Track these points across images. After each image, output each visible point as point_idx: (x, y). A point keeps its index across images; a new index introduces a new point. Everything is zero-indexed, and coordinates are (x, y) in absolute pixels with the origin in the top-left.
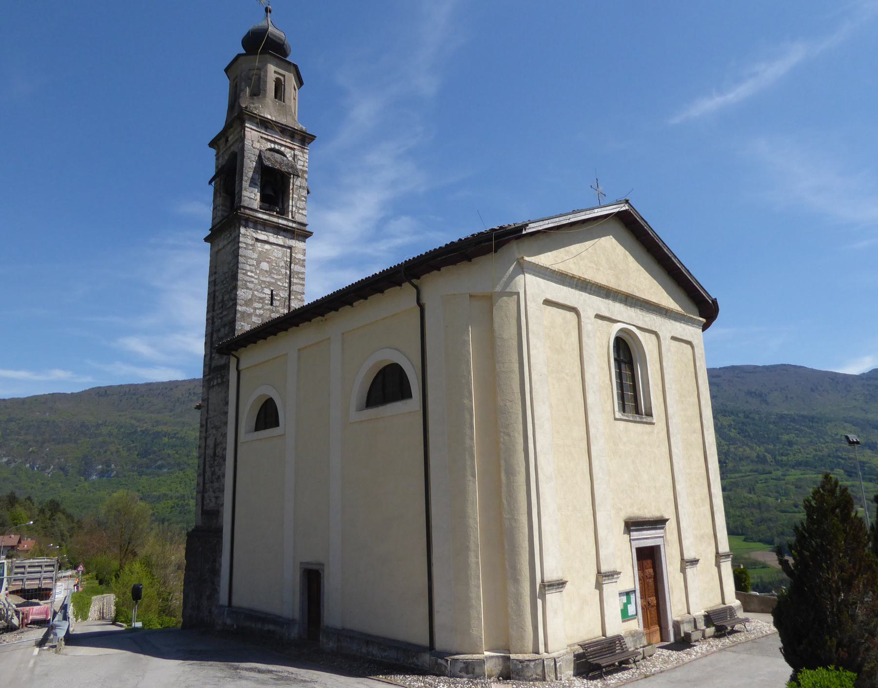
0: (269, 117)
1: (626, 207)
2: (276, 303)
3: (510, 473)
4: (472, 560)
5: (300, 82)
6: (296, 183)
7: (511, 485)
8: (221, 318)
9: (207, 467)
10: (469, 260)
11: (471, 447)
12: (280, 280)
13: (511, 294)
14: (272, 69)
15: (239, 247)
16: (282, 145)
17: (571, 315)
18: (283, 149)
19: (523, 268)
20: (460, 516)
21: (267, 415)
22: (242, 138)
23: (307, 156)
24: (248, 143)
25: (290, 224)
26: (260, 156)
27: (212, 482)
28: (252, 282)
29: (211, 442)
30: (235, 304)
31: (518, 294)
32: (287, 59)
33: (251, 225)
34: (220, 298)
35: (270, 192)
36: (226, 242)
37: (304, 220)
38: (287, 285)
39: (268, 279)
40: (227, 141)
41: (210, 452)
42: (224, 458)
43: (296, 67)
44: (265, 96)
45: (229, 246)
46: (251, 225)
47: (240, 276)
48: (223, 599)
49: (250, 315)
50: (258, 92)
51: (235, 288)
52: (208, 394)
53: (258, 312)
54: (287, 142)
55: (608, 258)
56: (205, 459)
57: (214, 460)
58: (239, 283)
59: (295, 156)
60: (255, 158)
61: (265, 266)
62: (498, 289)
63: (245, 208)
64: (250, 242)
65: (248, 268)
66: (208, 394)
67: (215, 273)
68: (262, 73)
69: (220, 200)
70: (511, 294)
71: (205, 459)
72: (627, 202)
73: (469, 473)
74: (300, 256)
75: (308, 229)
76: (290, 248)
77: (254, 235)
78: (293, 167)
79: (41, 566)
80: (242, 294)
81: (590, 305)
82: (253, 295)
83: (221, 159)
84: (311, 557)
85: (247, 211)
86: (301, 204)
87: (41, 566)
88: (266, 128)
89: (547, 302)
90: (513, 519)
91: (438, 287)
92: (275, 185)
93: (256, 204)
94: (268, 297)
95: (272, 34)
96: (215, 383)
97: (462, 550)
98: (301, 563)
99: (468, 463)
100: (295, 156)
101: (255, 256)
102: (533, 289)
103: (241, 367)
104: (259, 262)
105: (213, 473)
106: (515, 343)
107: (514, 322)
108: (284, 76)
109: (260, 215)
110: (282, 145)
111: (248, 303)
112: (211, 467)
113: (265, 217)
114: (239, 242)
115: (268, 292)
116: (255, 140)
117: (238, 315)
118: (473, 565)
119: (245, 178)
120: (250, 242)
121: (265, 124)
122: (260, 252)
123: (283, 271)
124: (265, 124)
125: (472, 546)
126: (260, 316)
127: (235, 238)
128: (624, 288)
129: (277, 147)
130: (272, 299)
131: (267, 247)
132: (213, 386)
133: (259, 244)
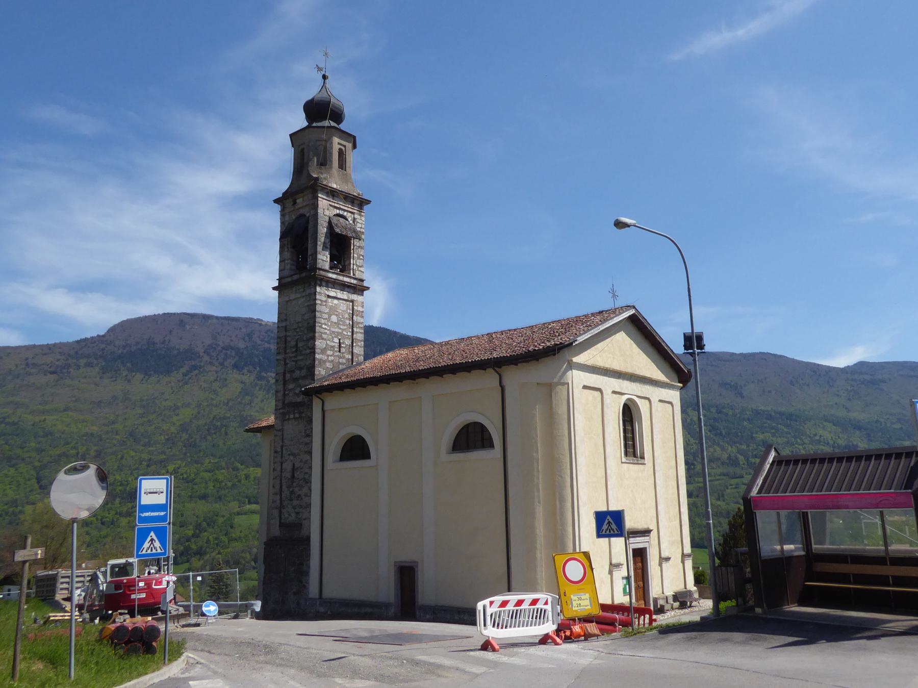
0: (335, 186)
1: (632, 312)
2: (343, 350)
3: (562, 500)
4: (538, 555)
5: (354, 147)
6: (355, 243)
7: (562, 507)
8: (296, 362)
9: (284, 487)
10: (537, 360)
11: (538, 485)
12: (344, 330)
13: (563, 384)
14: (336, 140)
15: (315, 304)
16: (345, 210)
17: (597, 394)
18: (345, 214)
19: (572, 366)
20: (531, 528)
21: (355, 449)
22: (315, 207)
23: (363, 219)
24: (320, 211)
25: (353, 281)
26: (330, 223)
27: (291, 500)
28: (325, 333)
29: (288, 466)
30: (314, 353)
31: (568, 384)
32: (342, 126)
33: (324, 284)
34: (293, 343)
35: (335, 252)
36: (298, 295)
37: (363, 277)
38: (350, 334)
39: (336, 330)
40: (295, 203)
41: (288, 475)
42: (308, 481)
43: (354, 137)
44: (331, 167)
45: (302, 300)
46: (324, 284)
47: (317, 328)
48: (313, 591)
49: (325, 362)
50: (324, 163)
51: (313, 338)
52: (283, 425)
53: (331, 358)
54: (348, 207)
55: (622, 350)
56: (281, 480)
57: (293, 482)
58: (317, 335)
59: (354, 219)
60: (326, 224)
61: (334, 318)
62: (556, 380)
63: (320, 269)
64: (324, 299)
65: (323, 321)
66: (283, 425)
67: (286, 320)
68: (328, 145)
69: (287, 255)
70: (563, 384)
71: (281, 480)
72: (634, 307)
73: (536, 500)
74: (360, 309)
75: (365, 284)
76: (352, 301)
77: (327, 293)
78: (355, 231)
79: (83, 576)
80: (319, 344)
81: (608, 384)
82: (327, 344)
83: (287, 218)
84: (405, 557)
85: (321, 272)
86: (359, 262)
87: (83, 576)
88: (333, 196)
89: (585, 387)
90: (564, 529)
91: (514, 377)
92: (341, 246)
93: (327, 266)
94: (337, 345)
95: (333, 106)
96: (292, 416)
97: (531, 550)
98: (395, 562)
99: (536, 494)
100: (354, 219)
101: (327, 310)
102: (577, 378)
103: (326, 408)
104: (330, 316)
105: (292, 492)
106: (566, 417)
107: (565, 403)
108: (345, 146)
109: (330, 275)
110: (345, 210)
111: (323, 351)
112: (288, 487)
113: (334, 276)
114: (315, 299)
115: (336, 340)
116: (326, 208)
117: (317, 362)
118: (539, 559)
119: (319, 243)
120: (324, 299)
121: (333, 194)
122: (331, 307)
123: (348, 322)
124: (333, 194)
125: (538, 546)
126: (332, 361)
127: (310, 295)
128: (629, 370)
129: (341, 212)
130: (340, 347)
131: (336, 301)
132: (289, 419)
133: (330, 300)
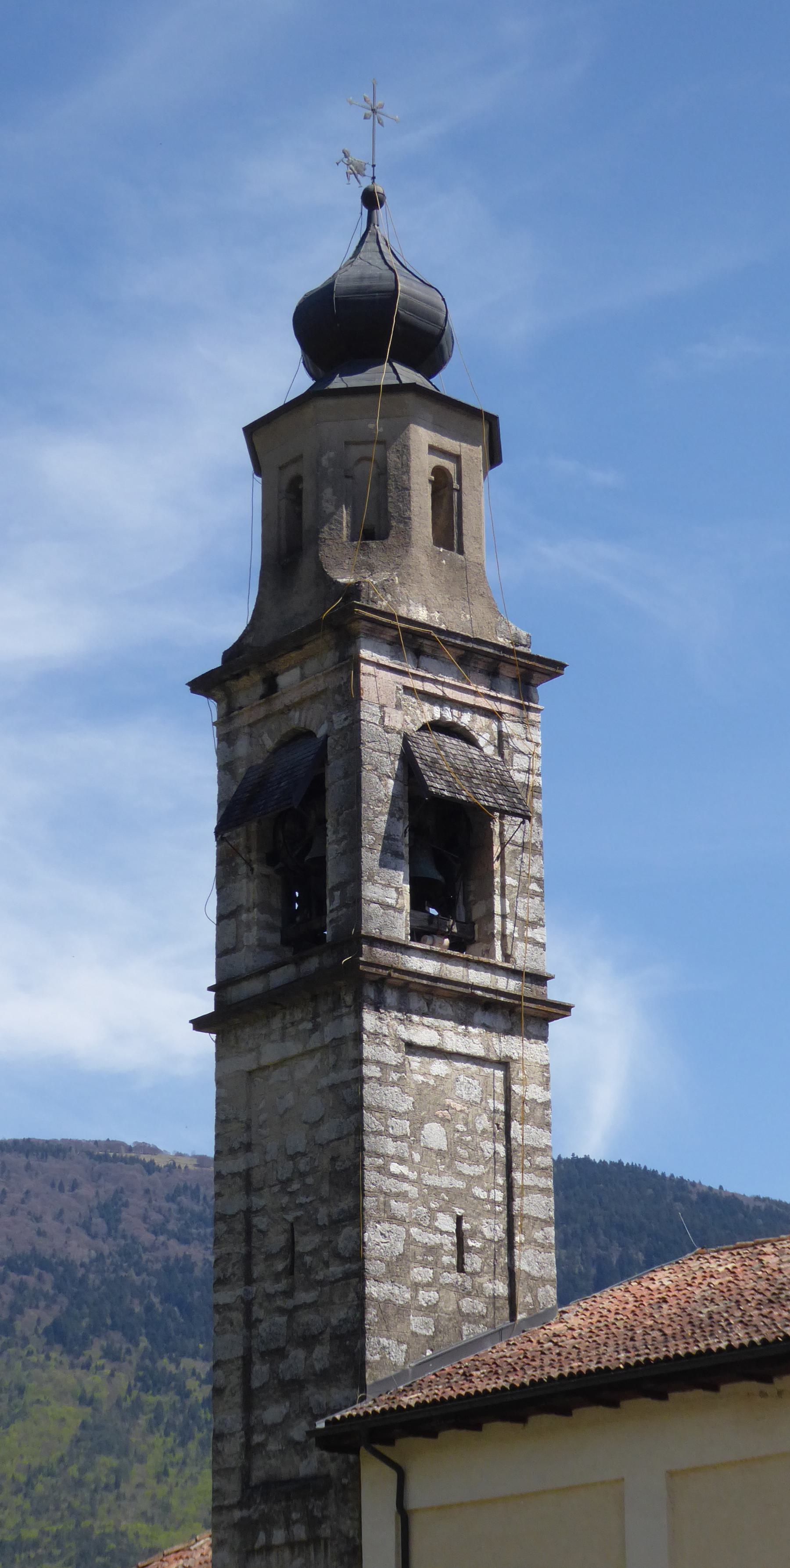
0: (421, 614)
2: (473, 1262)
5: (494, 457)
6: (511, 829)
8: (291, 1313)
14: (421, 437)
15: (360, 1080)
18: (466, 719)
22: (350, 698)
24: (369, 714)
25: (503, 983)
28: (402, 1196)
30: (360, 1275)
32: (447, 382)
33: (391, 997)
34: (277, 1240)
35: (432, 872)
36: (293, 1048)
37: (545, 963)
38: (499, 1196)
39: (445, 1181)
40: (271, 687)
43: (492, 421)
44: (406, 543)
45: (309, 1065)
46: (391, 997)
47: (371, 1178)
49: (403, 1311)
50: (378, 528)
51: (356, 1217)
54: (477, 692)
58: (369, 1203)
59: (502, 740)
60: (391, 765)
61: (435, 1135)
64: (392, 1057)
65: (390, 1147)
69: (247, 890)
74: (535, 1092)
75: (553, 992)
76: (504, 1064)
77: (405, 1033)
78: (505, 785)
80: (380, 1239)
82: (409, 1241)
83: (242, 747)
85: (383, 955)
86: (526, 907)
88: (418, 654)
92: (452, 845)
93: (400, 928)
94: (449, 1242)
95: (406, 306)
96: (279, 1536)
100: (502, 740)
101: (406, 1104)
103: (415, 1499)
104: (418, 1125)
108: (456, 458)
109: (415, 963)
111: (397, 1268)
113: (429, 966)
114: (359, 1061)
115: (446, 1223)
116: (390, 701)
117: (372, 1314)
119: (368, 839)
120: (392, 1057)
121: (416, 643)
122: (420, 1090)
123: (487, 1146)
124: (416, 643)
126: (431, 1309)
127: (338, 1043)
129: (450, 715)
130: (461, 1248)
131: (439, 1067)
132: (268, 1548)
133: (415, 1061)
